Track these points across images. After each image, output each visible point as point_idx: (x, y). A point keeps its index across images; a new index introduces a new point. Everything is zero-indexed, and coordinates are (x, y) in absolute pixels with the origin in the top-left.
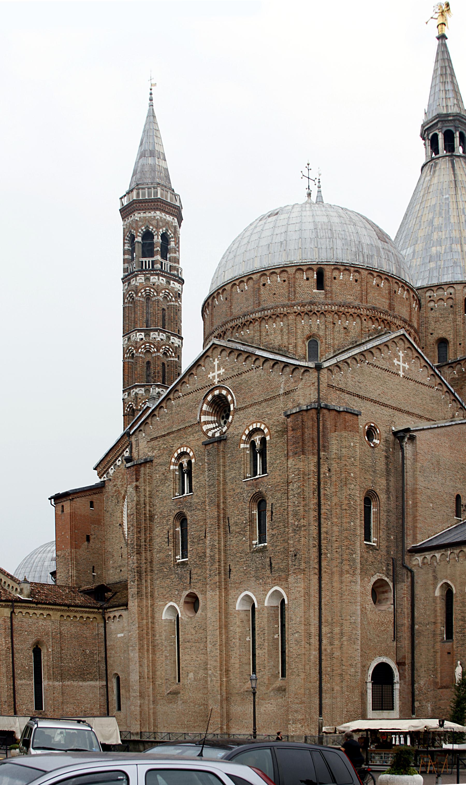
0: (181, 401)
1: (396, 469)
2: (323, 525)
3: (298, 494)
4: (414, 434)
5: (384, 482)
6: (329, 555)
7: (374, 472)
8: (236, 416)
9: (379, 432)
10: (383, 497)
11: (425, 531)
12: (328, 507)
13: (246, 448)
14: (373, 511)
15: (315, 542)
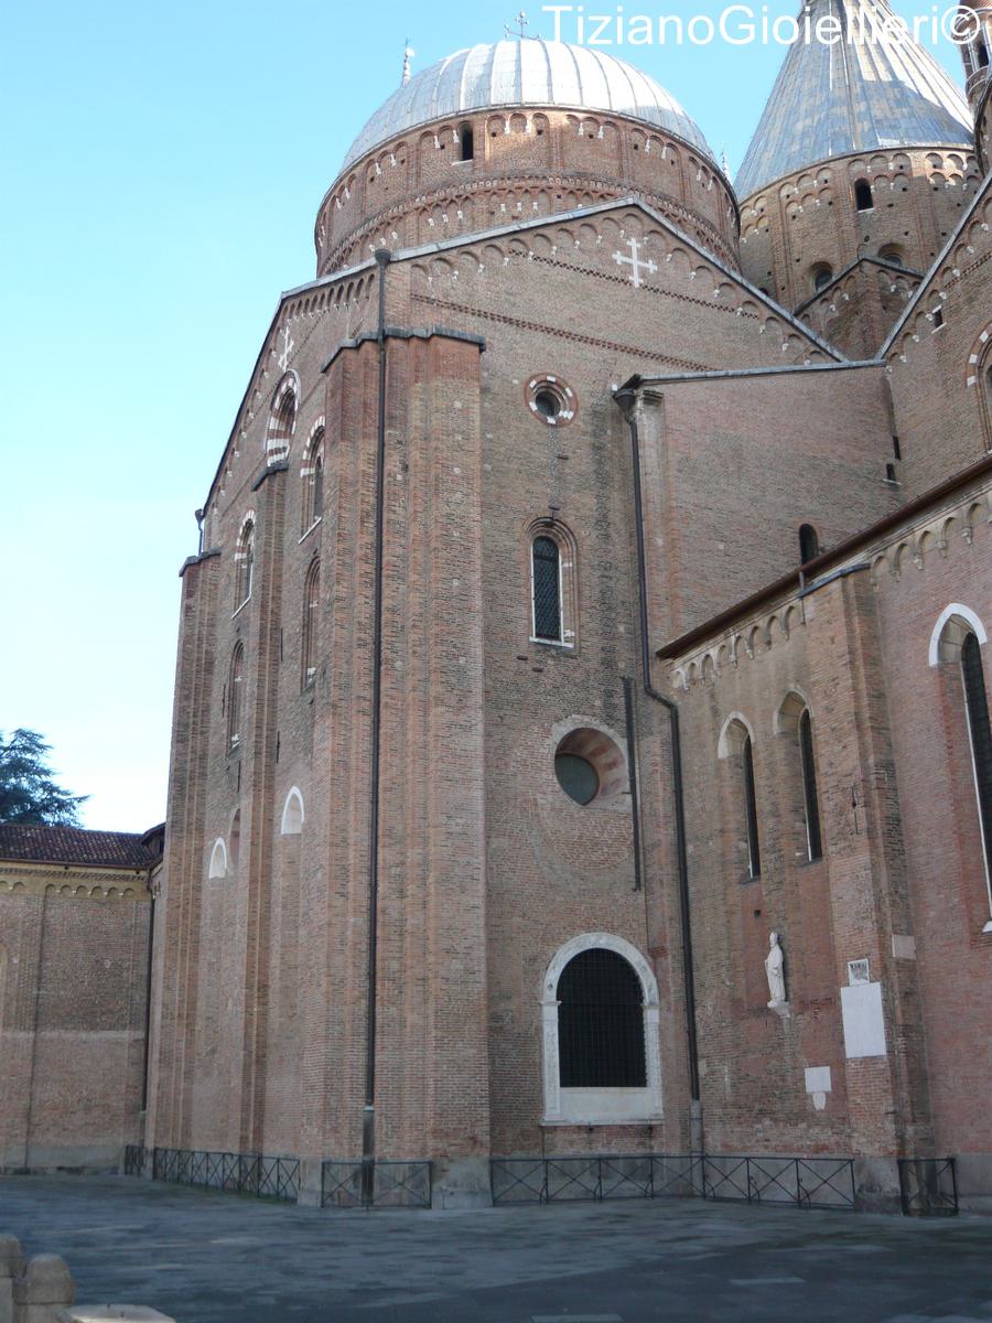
0: (252, 428)
1: (624, 471)
2: (386, 592)
3: (332, 529)
4: (657, 389)
5: (589, 502)
6: (398, 664)
7: (558, 478)
8: (301, 418)
9: (570, 394)
10: (587, 535)
11: (705, 606)
12: (400, 551)
13: (309, 476)
14: (564, 569)
15: (362, 635)
